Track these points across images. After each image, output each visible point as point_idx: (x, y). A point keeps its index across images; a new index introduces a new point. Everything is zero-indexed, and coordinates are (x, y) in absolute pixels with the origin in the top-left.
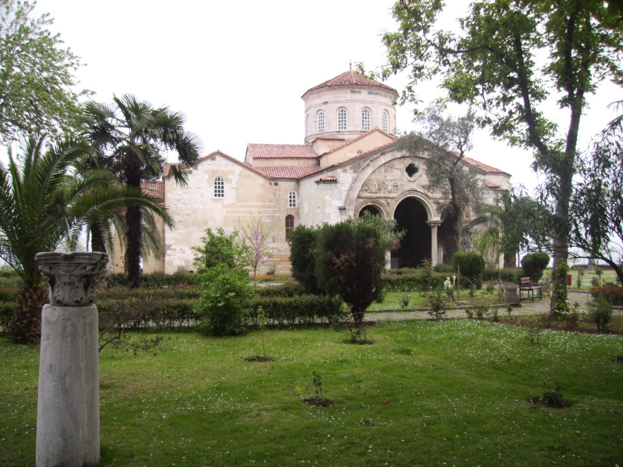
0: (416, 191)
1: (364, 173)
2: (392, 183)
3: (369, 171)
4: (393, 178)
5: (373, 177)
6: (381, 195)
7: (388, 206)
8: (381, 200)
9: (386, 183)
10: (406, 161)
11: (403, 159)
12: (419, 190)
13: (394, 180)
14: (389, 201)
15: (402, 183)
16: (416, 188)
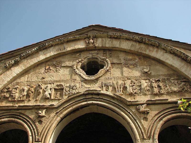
0: (98, 94)
1: (8, 73)
2: (54, 86)
3: (17, 70)
4: (58, 79)
5: (24, 79)
6: (32, 103)
7: (40, 122)
8: (27, 113)
9: (43, 87)
10: (82, 55)
11: (78, 54)
12: (104, 92)
13: (57, 81)
14: (43, 113)
15: (72, 84)
16: (99, 89)
